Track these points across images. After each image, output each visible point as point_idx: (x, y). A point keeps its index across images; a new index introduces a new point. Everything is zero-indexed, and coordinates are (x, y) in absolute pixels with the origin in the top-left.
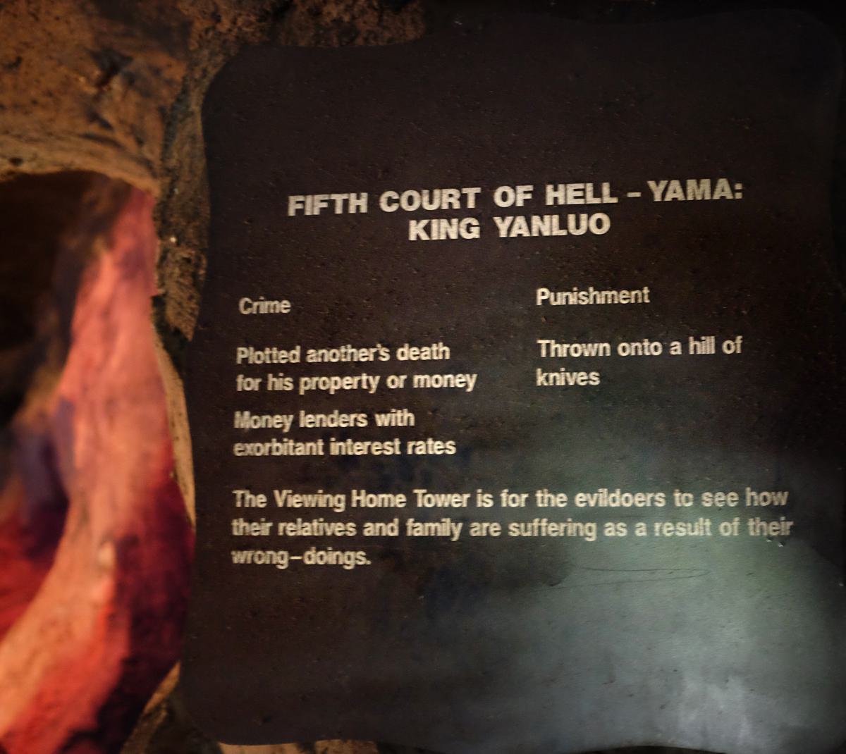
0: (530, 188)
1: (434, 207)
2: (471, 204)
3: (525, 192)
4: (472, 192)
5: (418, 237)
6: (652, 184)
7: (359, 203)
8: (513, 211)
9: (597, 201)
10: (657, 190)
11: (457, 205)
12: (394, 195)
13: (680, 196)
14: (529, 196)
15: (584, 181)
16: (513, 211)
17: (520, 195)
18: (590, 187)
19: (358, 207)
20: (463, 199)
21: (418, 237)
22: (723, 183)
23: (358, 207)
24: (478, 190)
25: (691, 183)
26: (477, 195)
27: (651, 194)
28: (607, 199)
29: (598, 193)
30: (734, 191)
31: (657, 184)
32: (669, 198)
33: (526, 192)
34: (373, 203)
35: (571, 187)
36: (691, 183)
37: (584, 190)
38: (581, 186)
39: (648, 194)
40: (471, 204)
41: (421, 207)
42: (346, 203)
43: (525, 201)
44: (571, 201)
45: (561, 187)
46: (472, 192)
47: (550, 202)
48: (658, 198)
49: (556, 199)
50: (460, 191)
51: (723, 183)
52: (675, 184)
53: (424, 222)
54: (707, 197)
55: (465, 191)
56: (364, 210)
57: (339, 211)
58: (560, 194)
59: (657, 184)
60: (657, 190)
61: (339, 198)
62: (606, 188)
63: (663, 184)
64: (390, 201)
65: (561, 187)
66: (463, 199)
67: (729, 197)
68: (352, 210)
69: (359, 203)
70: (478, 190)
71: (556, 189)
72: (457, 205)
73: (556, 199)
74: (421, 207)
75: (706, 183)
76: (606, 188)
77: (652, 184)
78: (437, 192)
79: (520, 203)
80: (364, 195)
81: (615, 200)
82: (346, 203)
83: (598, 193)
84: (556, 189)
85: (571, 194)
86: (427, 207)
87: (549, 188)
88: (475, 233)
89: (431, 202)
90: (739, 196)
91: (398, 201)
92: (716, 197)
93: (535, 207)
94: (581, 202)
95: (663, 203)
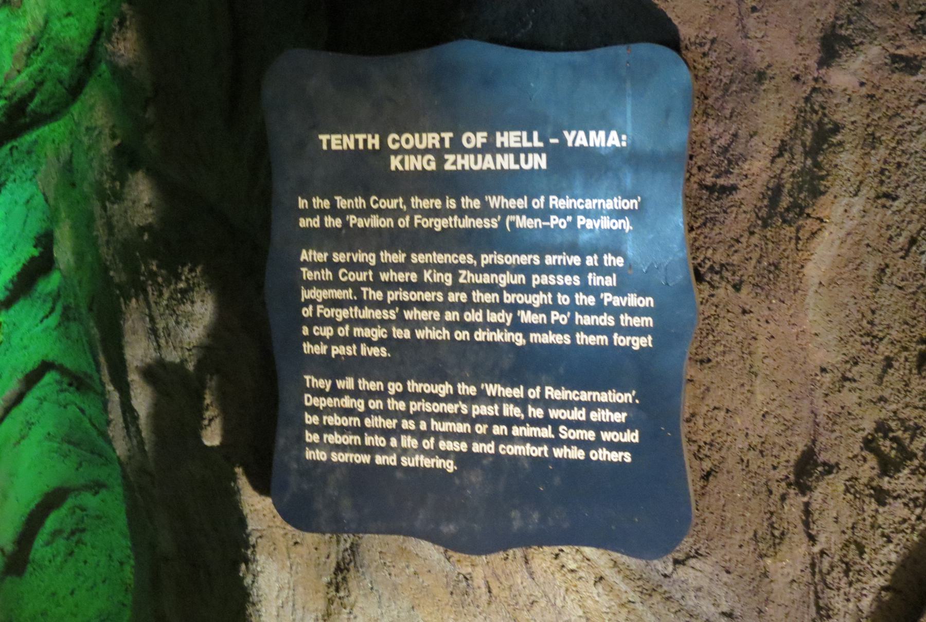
0: (485, 134)
1: (422, 147)
2: (447, 145)
3: (482, 137)
4: (447, 136)
5: (396, 167)
6: (566, 133)
7: (374, 142)
8: (475, 151)
9: (529, 145)
10: (569, 137)
11: (438, 146)
12: (397, 137)
13: (586, 144)
14: (485, 140)
15: (521, 130)
16: (475, 151)
17: (480, 138)
18: (525, 134)
19: (373, 145)
20: (442, 140)
21: (396, 167)
22: (614, 134)
23: (373, 145)
24: (451, 135)
25: (592, 134)
26: (451, 139)
27: (566, 141)
28: (537, 144)
29: (530, 139)
30: (621, 140)
31: (569, 133)
32: (577, 144)
33: (482, 137)
34: (383, 142)
35: (512, 134)
36: (592, 134)
37: (521, 137)
38: (518, 133)
39: (563, 141)
40: (447, 145)
41: (415, 146)
42: (365, 141)
43: (483, 144)
44: (513, 145)
45: (506, 134)
46: (447, 136)
47: (499, 145)
48: (570, 144)
49: (502, 143)
50: (440, 134)
51: (614, 134)
52: (582, 134)
53: (400, 157)
54: (603, 145)
55: (443, 135)
56: (377, 147)
57: (361, 146)
58: (505, 139)
59: (569, 133)
60: (569, 137)
61: (361, 137)
62: (536, 134)
63: (573, 133)
64: (394, 141)
65: (506, 134)
66: (442, 140)
67: (618, 145)
68: (370, 147)
69: (374, 142)
70: (451, 135)
71: (502, 135)
72: (438, 146)
73: (502, 143)
74: (415, 146)
75: (602, 133)
76: (536, 134)
77: (566, 133)
78: (424, 135)
79: (479, 146)
80: (377, 136)
81: (541, 145)
82: (365, 141)
83: (530, 139)
84: (502, 135)
85: (512, 139)
86: (419, 146)
87: (498, 134)
88: (433, 166)
89: (421, 142)
90: (624, 144)
91: (399, 141)
92: (609, 145)
93: (489, 148)
94: (519, 145)
95: (574, 147)
